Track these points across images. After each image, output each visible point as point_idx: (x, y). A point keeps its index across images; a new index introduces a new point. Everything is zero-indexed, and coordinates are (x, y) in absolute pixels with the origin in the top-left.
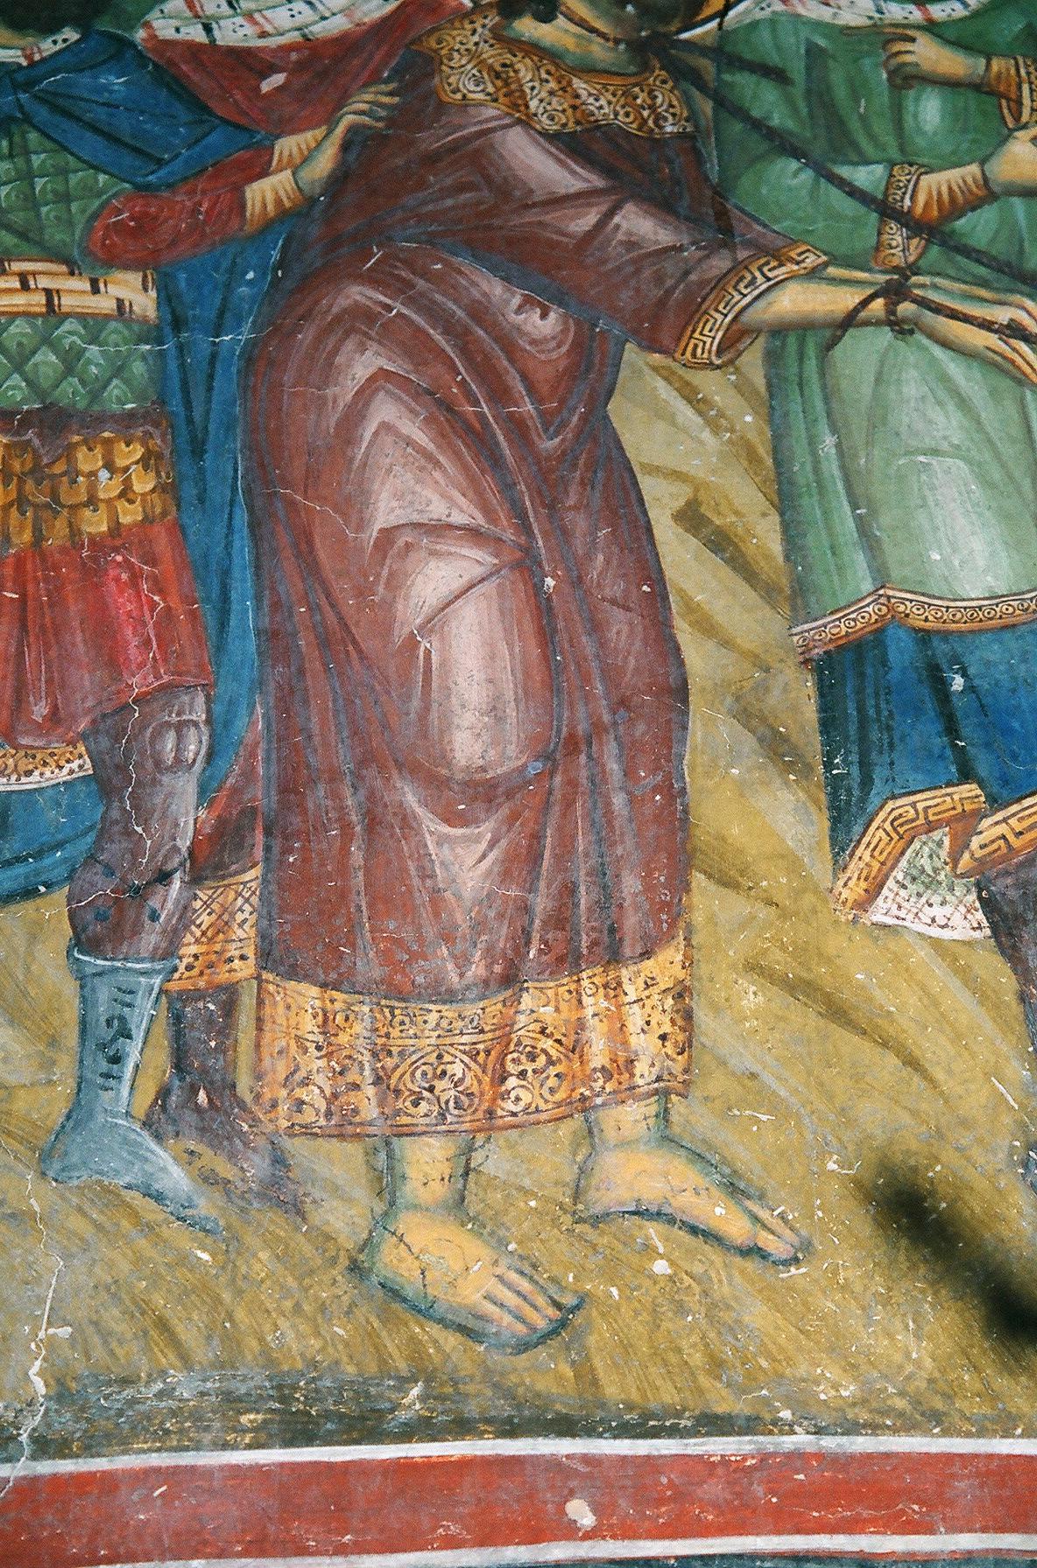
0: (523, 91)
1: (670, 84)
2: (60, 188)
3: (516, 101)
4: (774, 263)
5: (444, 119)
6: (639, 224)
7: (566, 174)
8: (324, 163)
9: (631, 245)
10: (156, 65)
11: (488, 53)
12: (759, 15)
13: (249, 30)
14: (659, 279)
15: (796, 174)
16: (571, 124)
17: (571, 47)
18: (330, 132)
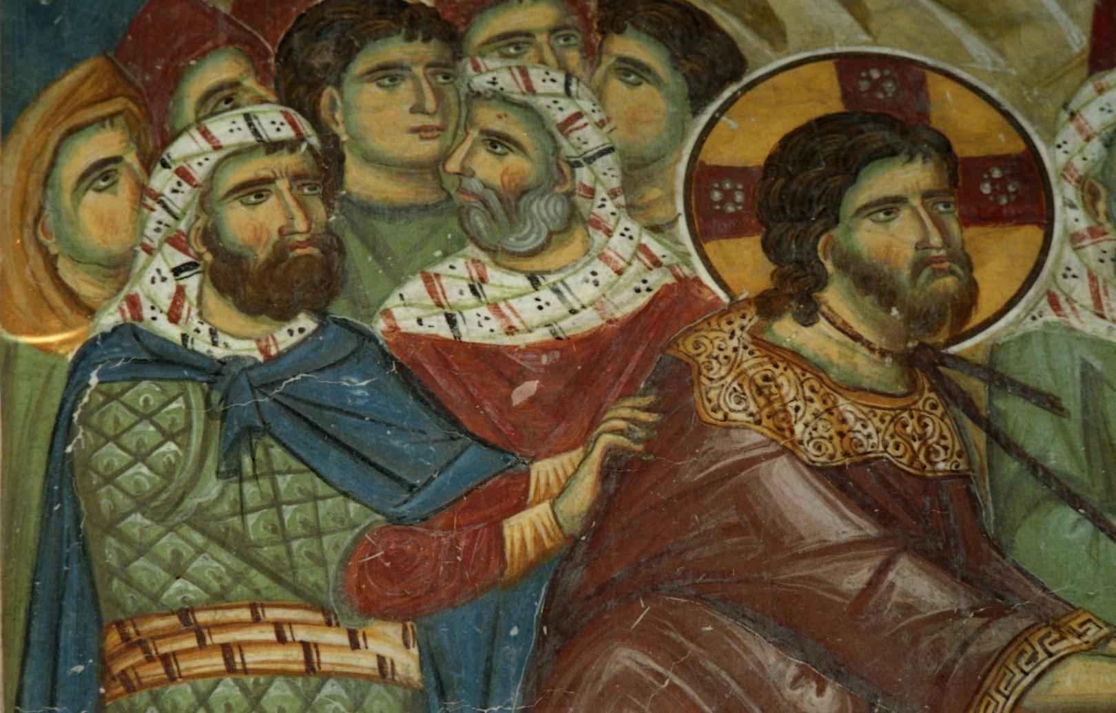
0: (785, 411)
1: (939, 412)
2: (310, 517)
3: (783, 428)
4: (1055, 636)
5: (707, 444)
6: (914, 583)
7: (838, 520)
8: (583, 494)
9: (908, 609)
10: (400, 366)
11: (749, 362)
12: (1030, 326)
13: (495, 323)
14: (936, 651)
15: (1074, 527)
16: (839, 456)
17: (835, 358)
18: (587, 455)
